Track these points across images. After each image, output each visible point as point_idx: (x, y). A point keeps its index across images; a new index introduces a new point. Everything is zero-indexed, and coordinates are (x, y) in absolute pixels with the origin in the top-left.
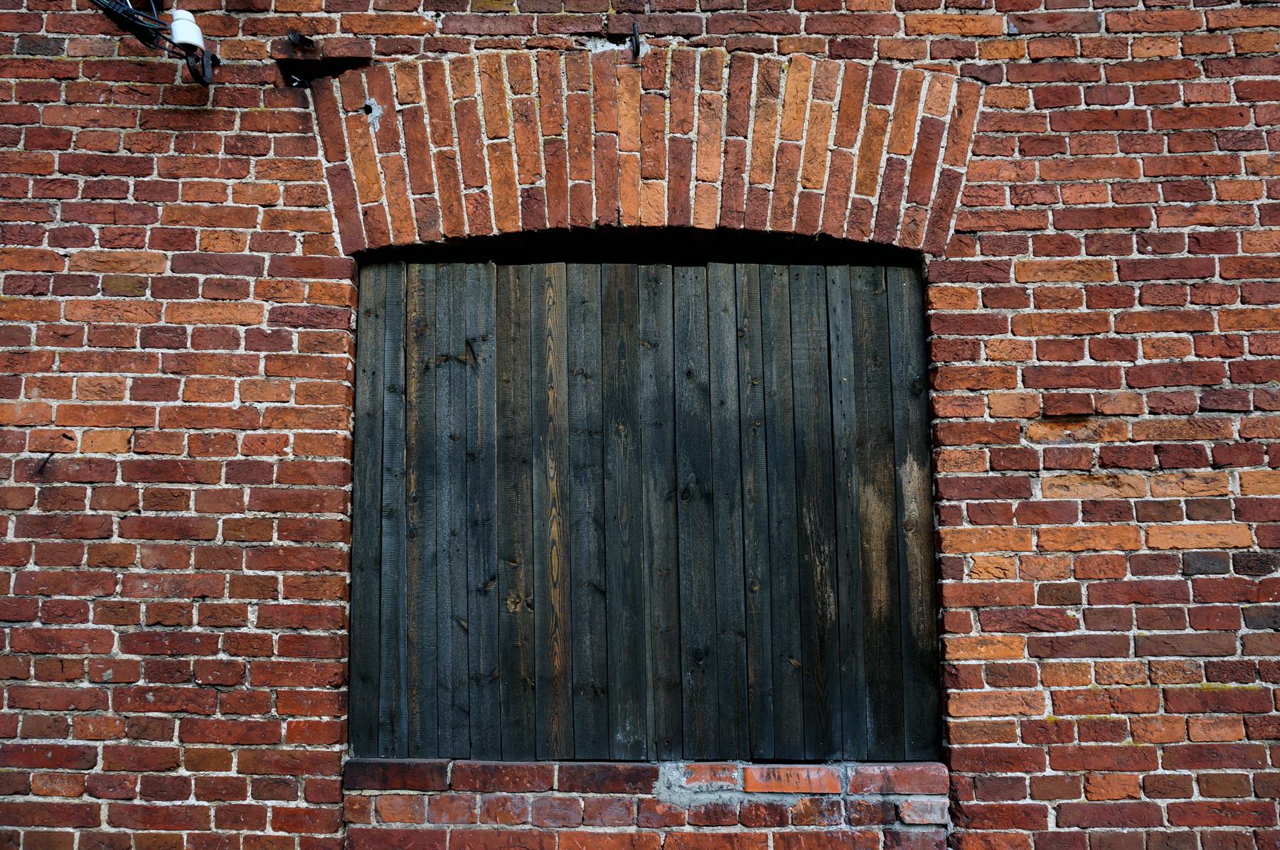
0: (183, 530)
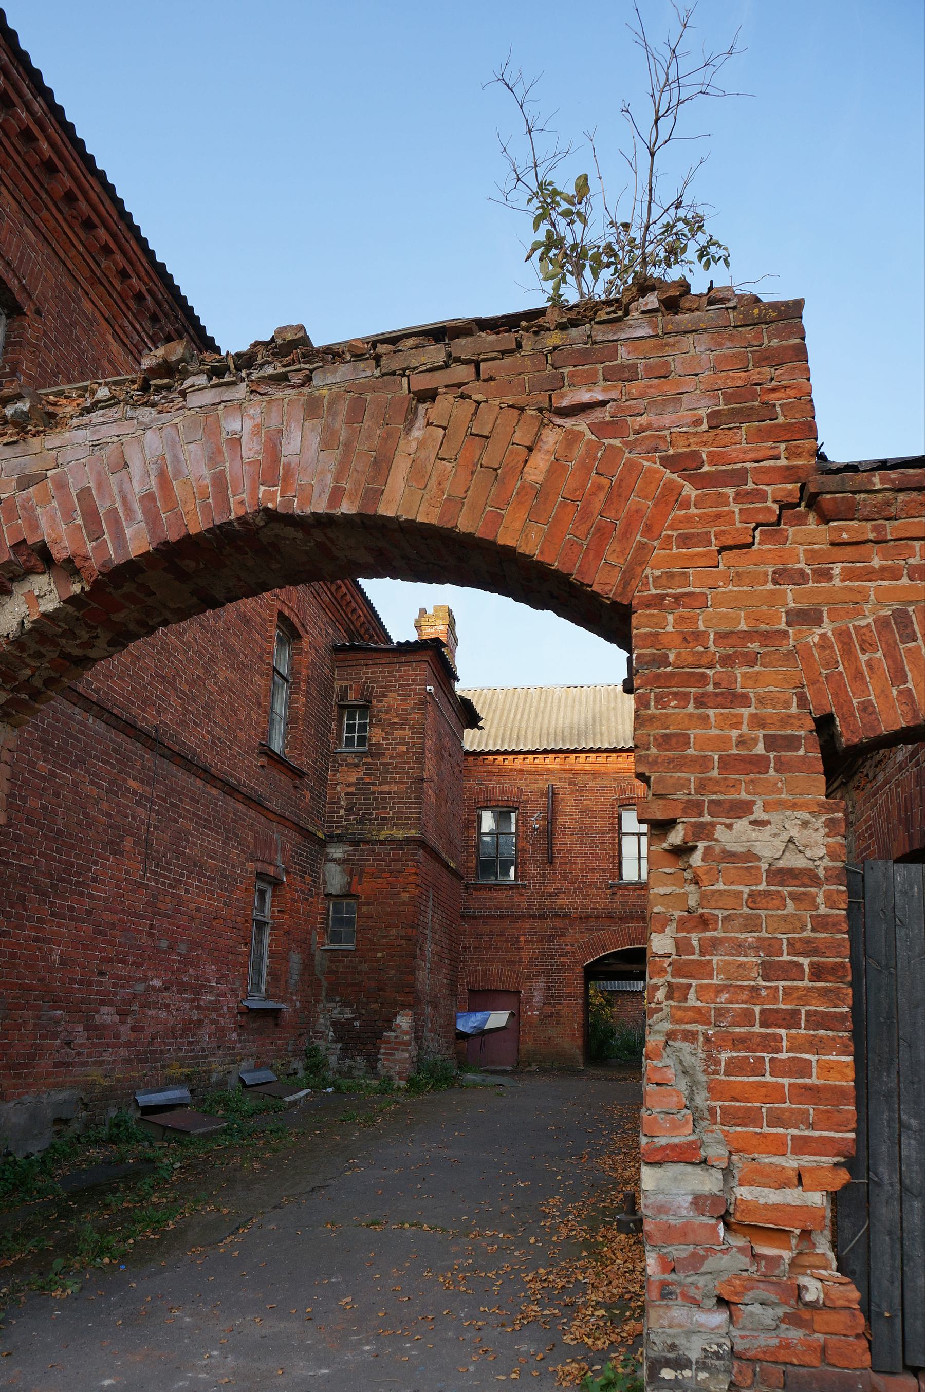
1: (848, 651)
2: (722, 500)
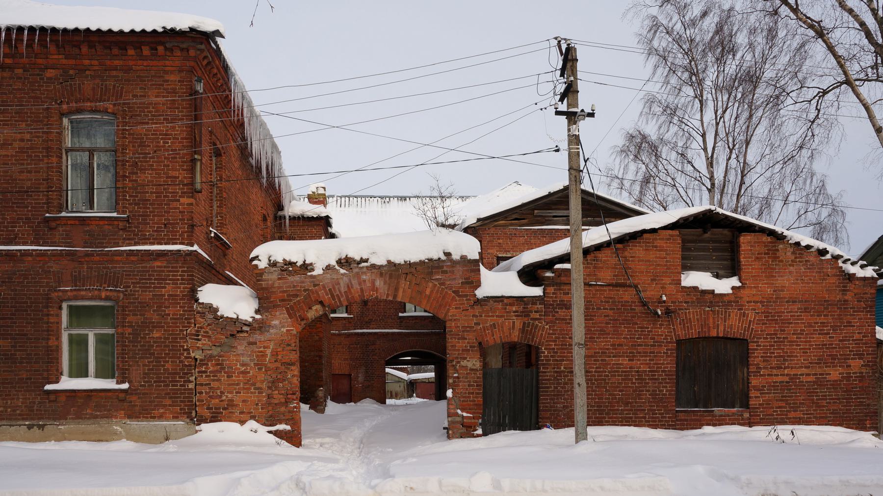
0: (656, 379)
1: (484, 330)
2: (463, 300)
